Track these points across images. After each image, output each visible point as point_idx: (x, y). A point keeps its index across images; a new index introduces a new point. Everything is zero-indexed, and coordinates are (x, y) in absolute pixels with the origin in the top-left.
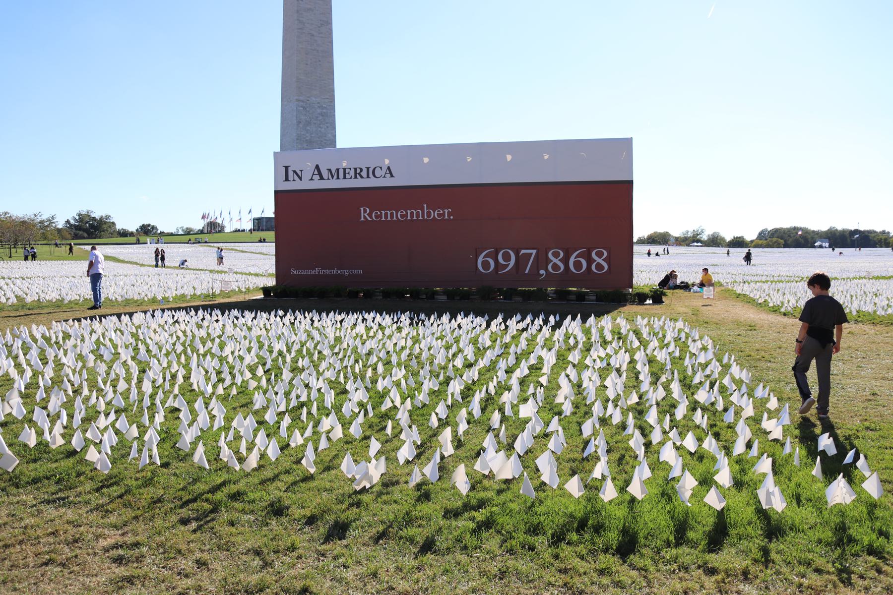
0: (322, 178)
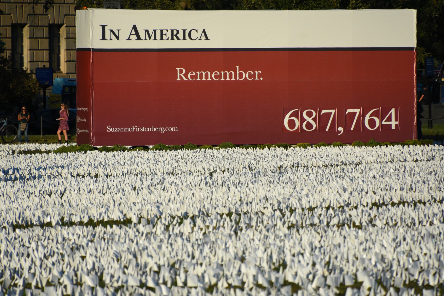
0: (139, 38)
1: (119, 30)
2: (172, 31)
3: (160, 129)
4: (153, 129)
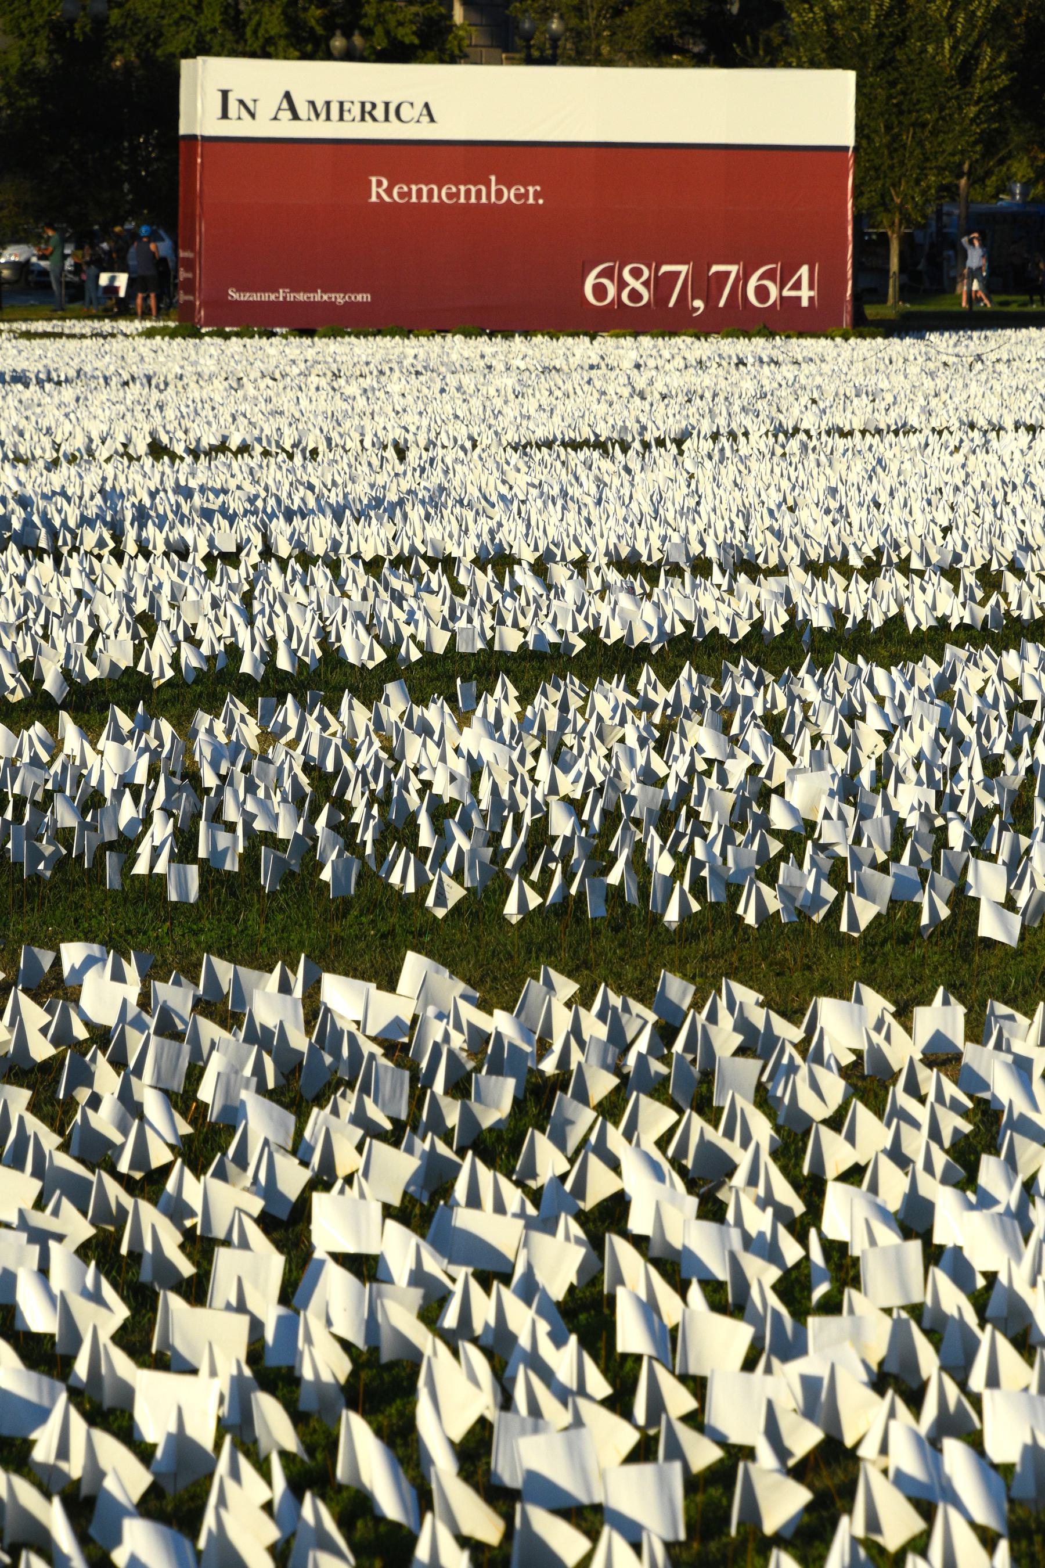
0: (296, 117)
2: (363, 104)
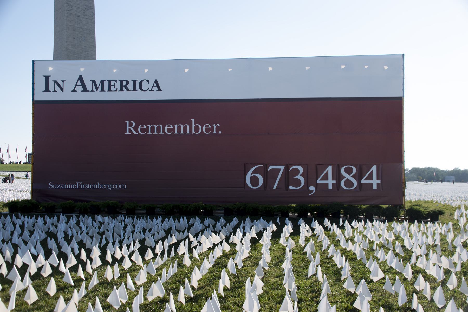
0: (85, 89)
1: (63, 81)
3: (107, 186)
4: (100, 186)
